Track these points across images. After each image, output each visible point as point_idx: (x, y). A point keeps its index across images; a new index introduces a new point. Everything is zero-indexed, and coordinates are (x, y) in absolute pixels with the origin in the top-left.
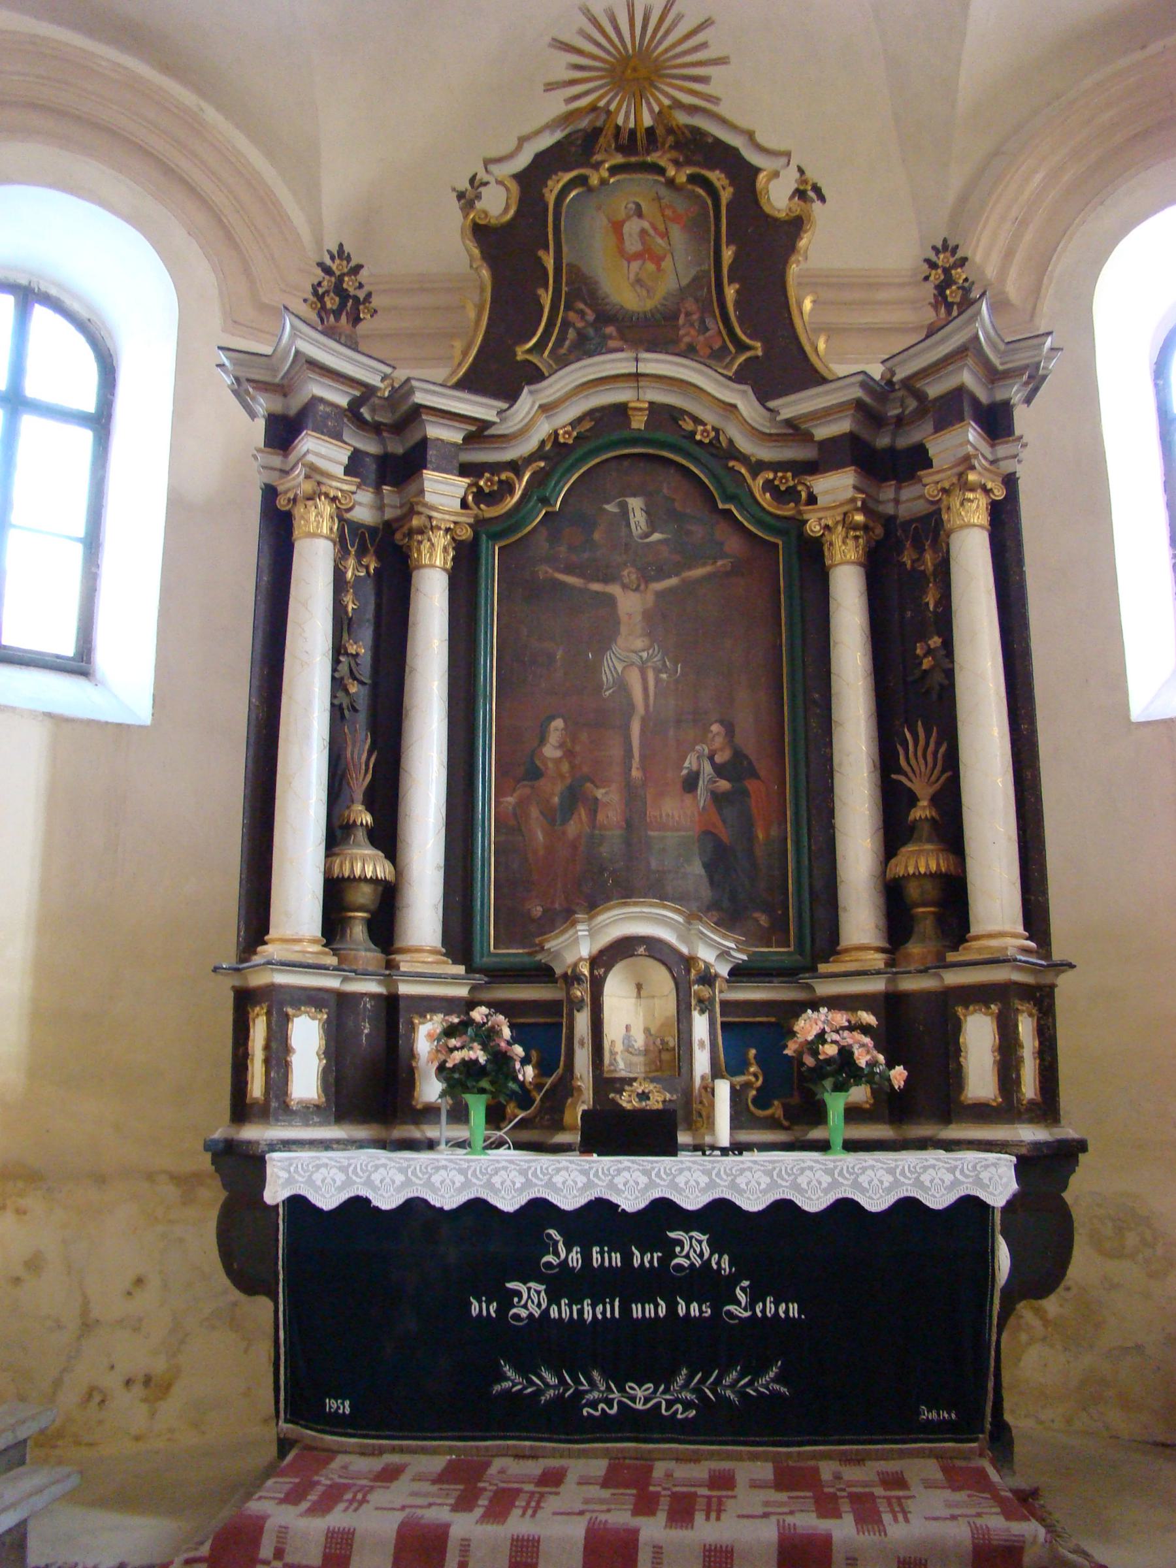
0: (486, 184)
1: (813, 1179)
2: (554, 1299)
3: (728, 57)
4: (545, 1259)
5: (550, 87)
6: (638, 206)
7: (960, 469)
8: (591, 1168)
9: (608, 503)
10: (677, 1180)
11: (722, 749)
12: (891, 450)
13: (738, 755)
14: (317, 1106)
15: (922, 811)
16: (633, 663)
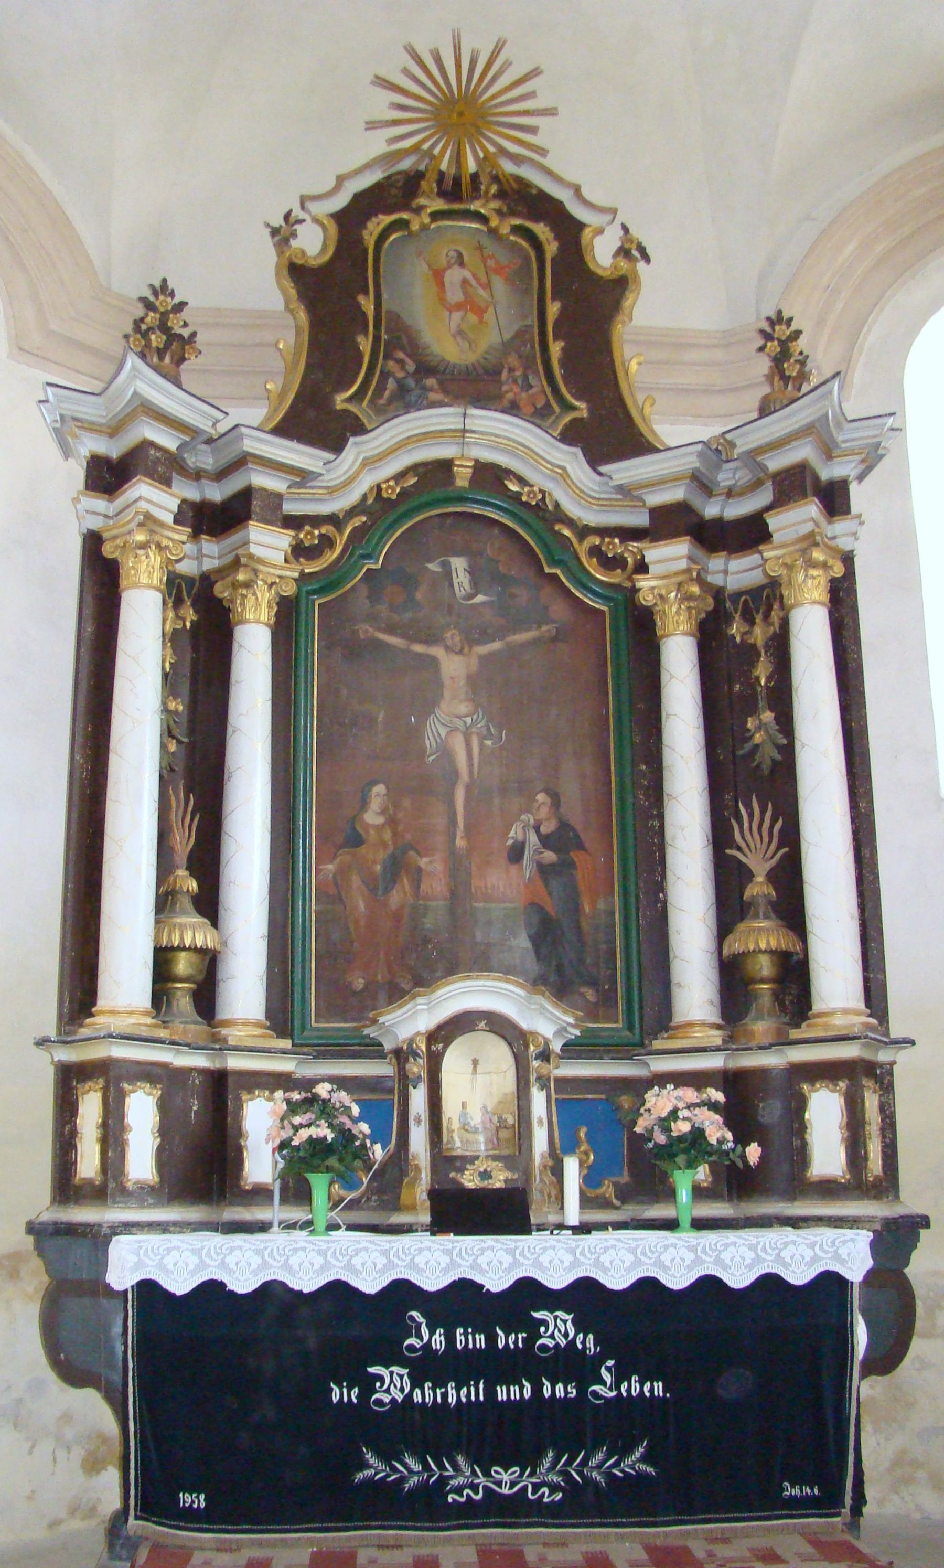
0: (301, 221)
1: (676, 1259)
2: (417, 1382)
3: (556, 109)
4: (408, 1342)
5: (372, 125)
6: (460, 255)
7: (803, 545)
8: (454, 1248)
9: (430, 561)
10: (541, 1259)
11: (546, 820)
12: (719, 522)
13: (564, 826)
14: (152, 1188)
15: (759, 888)
16: (456, 729)
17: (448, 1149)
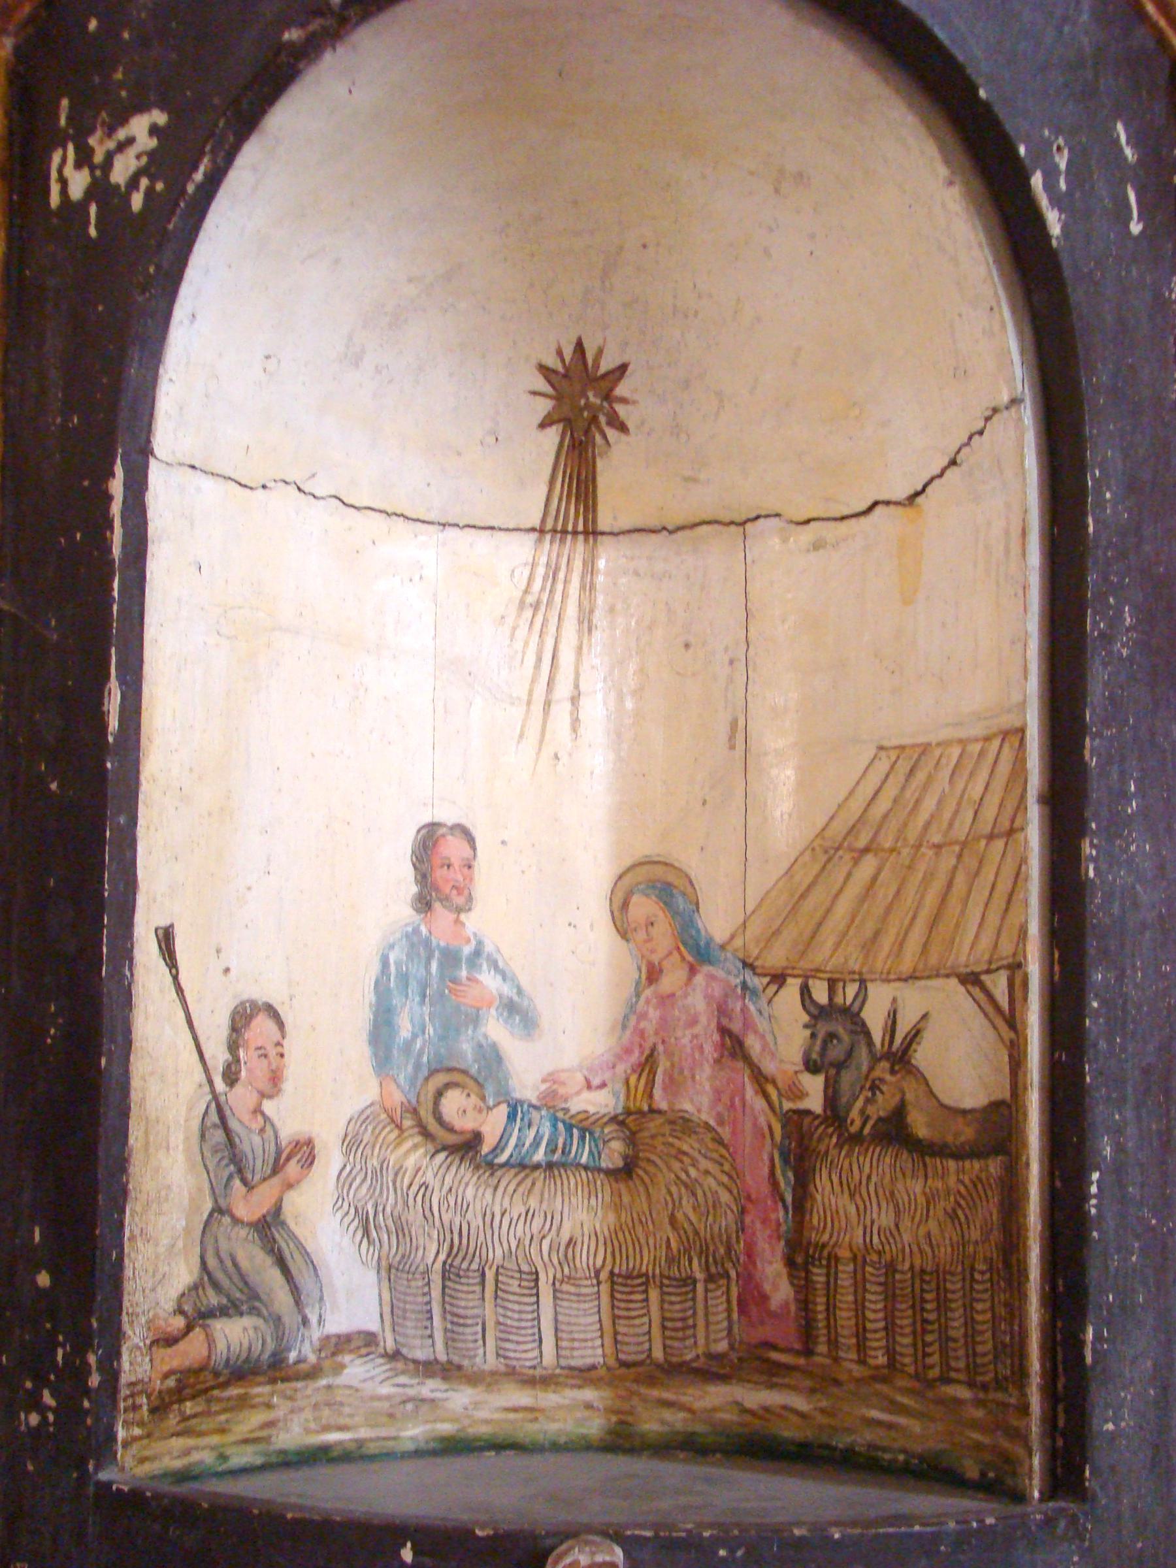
17: (202, 1387)
